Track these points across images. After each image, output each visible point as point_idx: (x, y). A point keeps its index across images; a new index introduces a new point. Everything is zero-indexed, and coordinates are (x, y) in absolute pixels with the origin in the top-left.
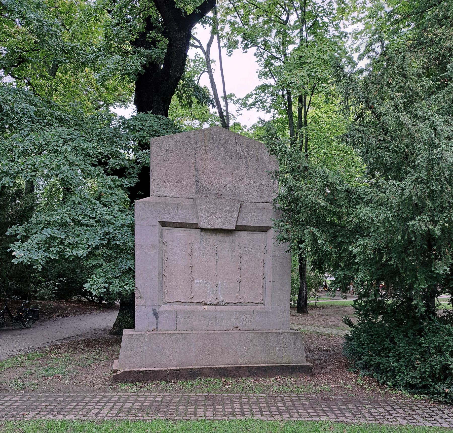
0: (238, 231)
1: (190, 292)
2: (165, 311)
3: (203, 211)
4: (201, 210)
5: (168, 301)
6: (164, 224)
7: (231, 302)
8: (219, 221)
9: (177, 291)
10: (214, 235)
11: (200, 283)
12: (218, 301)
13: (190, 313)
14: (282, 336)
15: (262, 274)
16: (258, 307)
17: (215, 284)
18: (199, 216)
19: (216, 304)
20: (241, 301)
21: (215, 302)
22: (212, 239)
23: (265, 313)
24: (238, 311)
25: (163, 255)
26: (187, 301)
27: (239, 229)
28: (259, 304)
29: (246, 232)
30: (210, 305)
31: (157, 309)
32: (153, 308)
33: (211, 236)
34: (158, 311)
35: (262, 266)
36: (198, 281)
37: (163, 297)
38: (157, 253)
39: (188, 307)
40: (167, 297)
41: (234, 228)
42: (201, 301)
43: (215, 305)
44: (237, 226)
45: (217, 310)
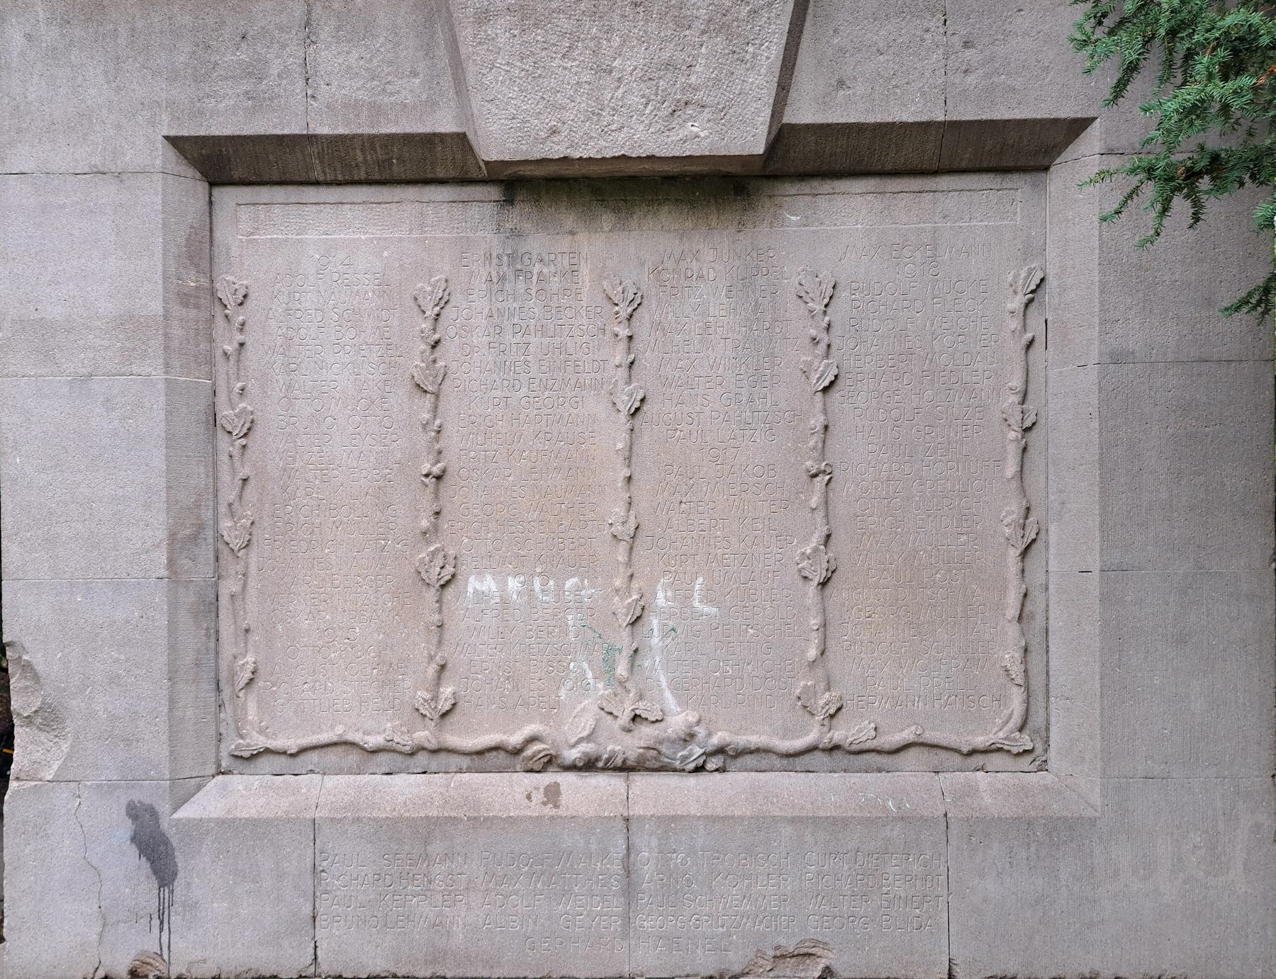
0: (804, 176)
1: (432, 670)
2: (228, 825)
3: (499, 29)
4: (484, 16)
5: (261, 742)
6: (221, 163)
7: (754, 740)
8: (635, 100)
9: (329, 661)
10: (607, 220)
11: (504, 601)
12: (646, 733)
13: (417, 838)
15: (1013, 510)
16: (991, 788)
17: (623, 607)
18: (471, 70)
19: (632, 755)
20: (838, 735)
21: (629, 746)
22: (599, 256)
23: (1047, 835)
24: (815, 821)
25: (222, 397)
26: (405, 741)
27: (801, 159)
28: (996, 760)
30: (589, 765)
31: (163, 808)
32: (137, 796)
33: (582, 237)
36: (488, 584)
37: (227, 714)
38: (159, 376)
39: (406, 790)
40: (252, 713)
41: (749, 138)
42: (515, 739)
43: (625, 768)
44: (783, 136)
45: (636, 810)
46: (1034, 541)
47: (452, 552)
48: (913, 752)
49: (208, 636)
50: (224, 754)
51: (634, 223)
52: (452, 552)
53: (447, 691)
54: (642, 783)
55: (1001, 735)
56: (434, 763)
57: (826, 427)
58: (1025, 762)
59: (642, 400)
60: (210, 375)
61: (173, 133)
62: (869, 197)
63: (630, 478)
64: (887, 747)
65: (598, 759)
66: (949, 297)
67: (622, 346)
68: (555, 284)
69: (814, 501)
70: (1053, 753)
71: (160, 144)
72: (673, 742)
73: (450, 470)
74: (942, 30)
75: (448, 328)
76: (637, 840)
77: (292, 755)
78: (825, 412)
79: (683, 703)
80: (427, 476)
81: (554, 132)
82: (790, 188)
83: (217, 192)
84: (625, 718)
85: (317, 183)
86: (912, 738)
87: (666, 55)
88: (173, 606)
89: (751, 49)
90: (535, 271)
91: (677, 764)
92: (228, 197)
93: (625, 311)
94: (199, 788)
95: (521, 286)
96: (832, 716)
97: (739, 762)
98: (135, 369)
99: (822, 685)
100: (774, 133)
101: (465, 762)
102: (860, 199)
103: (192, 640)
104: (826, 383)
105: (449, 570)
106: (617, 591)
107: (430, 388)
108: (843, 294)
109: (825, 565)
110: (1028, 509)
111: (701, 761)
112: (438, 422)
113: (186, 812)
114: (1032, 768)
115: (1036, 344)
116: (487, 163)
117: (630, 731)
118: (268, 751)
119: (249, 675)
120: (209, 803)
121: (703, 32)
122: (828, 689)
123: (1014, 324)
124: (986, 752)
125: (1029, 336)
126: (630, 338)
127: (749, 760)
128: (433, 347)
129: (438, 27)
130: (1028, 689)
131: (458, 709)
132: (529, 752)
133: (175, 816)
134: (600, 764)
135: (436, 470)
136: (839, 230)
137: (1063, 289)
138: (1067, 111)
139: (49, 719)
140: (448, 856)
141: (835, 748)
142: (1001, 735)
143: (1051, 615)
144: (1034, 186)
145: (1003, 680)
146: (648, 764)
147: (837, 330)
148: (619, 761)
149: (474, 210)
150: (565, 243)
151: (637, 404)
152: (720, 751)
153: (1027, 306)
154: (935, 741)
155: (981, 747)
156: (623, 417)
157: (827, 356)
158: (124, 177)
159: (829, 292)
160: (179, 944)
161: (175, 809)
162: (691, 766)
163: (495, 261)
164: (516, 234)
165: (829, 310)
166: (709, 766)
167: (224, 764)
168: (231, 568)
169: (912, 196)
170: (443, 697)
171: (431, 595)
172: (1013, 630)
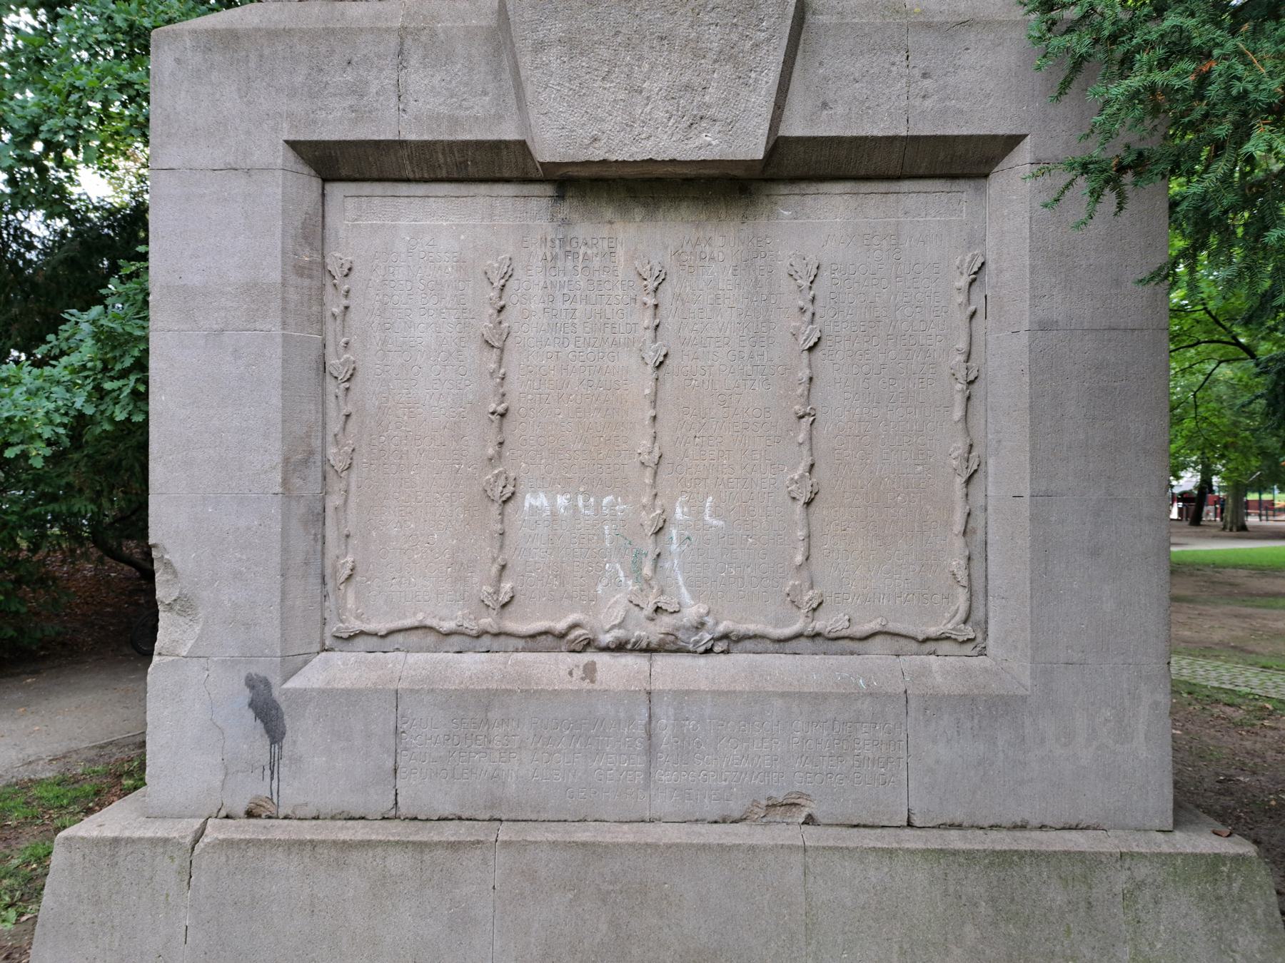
0: (795, 179)
1: (495, 569)
2: (328, 694)
3: (552, 56)
4: (539, 47)
5: (357, 625)
6: (331, 163)
7: (752, 628)
8: (660, 115)
9: (412, 563)
10: (638, 213)
11: (554, 514)
12: (666, 622)
13: (480, 705)
14: (1121, 881)
15: (959, 446)
16: (941, 670)
17: (649, 520)
18: (529, 90)
19: (655, 640)
20: (819, 625)
22: (633, 243)
24: (801, 695)
25: (330, 349)
26: (472, 626)
28: (945, 647)
29: (848, 186)
30: (620, 647)
31: (275, 680)
32: (255, 670)
33: (619, 226)
34: (285, 688)
35: (959, 399)
36: (541, 500)
37: (330, 603)
38: (277, 331)
40: (351, 603)
41: (754, 148)
42: (561, 626)
43: (649, 650)
44: (778, 146)
46: (976, 471)
47: (512, 475)
48: (878, 639)
49: (316, 540)
50: (328, 634)
51: (660, 215)
52: (512, 475)
53: (506, 586)
54: (661, 660)
55: (949, 626)
56: (496, 643)
57: (811, 379)
58: (968, 649)
59: (666, 356)
60: (321, 332)
61: (292, 138)
62: (846, 197)
63: (655, 417)
64: (858, 635)
65: (627, 642)
66: (909, 277)
67: (650, 312)
68: (596, 262)
69: (801, 437)
70: (990, 641)
71: (282, 147)
72: (688, 629)
73: (512, 409)
74: (905, 64)
75: (511, 297)
76: (657, 710)
77: (382, 637)
78: (810, 366)
79: (696, 597)
80: (493, 413)
81: (595, 140)
82: (784, 189)
83: (328, 186)
84: (649, 609)
85: (408, 180)
86: (878, 628)
87: (685, 79)
88: (286, 517)
89: (753, 75)
90: (581, 253)
91: (691, 647)
92: (337, 191)
93: (652, 284)
94: (306, 663)
95: (570, 264)
96: (814, 610)
97: (740, 645)
98: (258, 325)
99: (807, 584)
100: (771, 143)
101: (521, 643)
102: (839, 198)
103: (301, 544)
104: (811, 344)
105: (510, 489)
106: (644, 507)
107: (496, 344)
108: (825, 274)
109: (809, 489)
110: (971, 446)
111: (709, 645)
112: (502, 371)
113: (292, 684)
114: (974, 653)
115: (978, 315)
116: (542, 164)
117: (653, 620)
118: (362, 633)
119: (348, 572)
120: (313, 677)
121: (716, 61)
122: (812, 587)
123: (961, 298)
124: (937, 639)
125: (972, 308)
126: (656, 306)
127: (748, 644)
128: (500, 311)
129: (504, 56)
130: (970, 590)
131: (516, 600)
132: (572, 636)
133: (285, 686)
134: (629, 647)
135: (500, 409)
136: (822, 222)
137: (1000, 271)
138: (1004, 129)
139: (185, 605)
140: (504, 721)
141: (817, 635)
142: (949, 626)
143: (990, 531)
144: (977, 189)
145: (951, 581)
146: (667, 647)
147: (818, 302)
148: (644, 645)
149: (533, 203)
150: (605, 231)
151: (661, 359)
152: (725, 636)
153: (971, 284)
154: (897, 631)
155: (933, 635)
156: (650, 369)
157: (812, 322)
158: (252, 172)
159: (814, 271)
160: (286, 791)
161: (285, 681)
162: (702, 649)
163: (549, 244)
164: (566, 222)
165: (814, 286)
166: (716, 649)
167: (327, 643)
168: (336, 486)
169: (879, 196)
170: (503, 591)
171: (495, 509)
172: (959, 543)
